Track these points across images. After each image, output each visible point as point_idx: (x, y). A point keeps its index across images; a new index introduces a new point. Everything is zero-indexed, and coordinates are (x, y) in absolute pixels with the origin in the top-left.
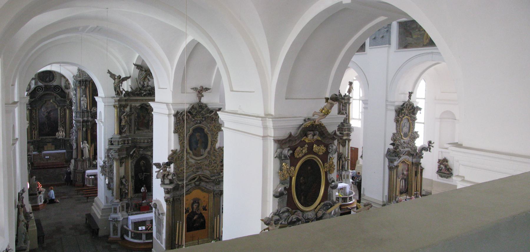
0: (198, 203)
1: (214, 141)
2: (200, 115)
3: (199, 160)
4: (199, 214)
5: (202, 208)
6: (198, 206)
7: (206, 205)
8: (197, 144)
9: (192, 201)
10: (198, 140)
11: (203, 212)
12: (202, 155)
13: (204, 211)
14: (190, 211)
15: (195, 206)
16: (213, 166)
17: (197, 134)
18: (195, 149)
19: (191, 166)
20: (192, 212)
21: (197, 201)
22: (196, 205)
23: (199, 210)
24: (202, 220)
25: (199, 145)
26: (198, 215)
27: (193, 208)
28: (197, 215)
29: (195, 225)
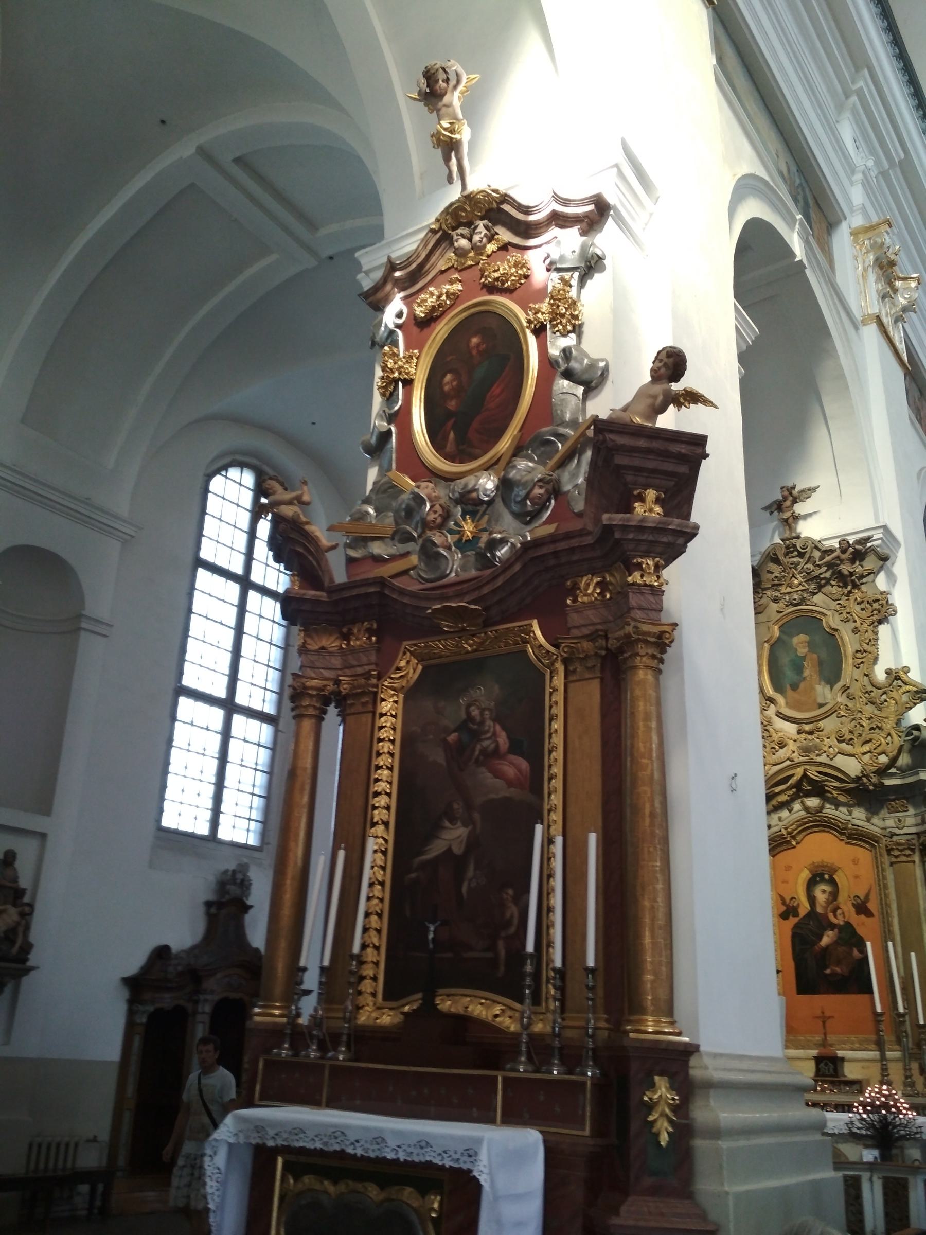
0: (832, 882)
1: (865, 651)
2: (798, 576)
3: (808, 721)
4: (841, 929)
5: (850, 904)
6: (834, 895)
7: (867, 896)
8: (798, 668)
9: (805, 875)
10: (804, 658)
11: (857, 921)
12: (821, 706)
13: (862, 917)
14: (803, 912)
15: (821, 893)
16: (870, 740)
17: (799, 641)
18: (795, 687)
19: (782, 745)
20: (812, 914)
21: (826, 877)
22: (824, 891)
23: (839, 911)
24: (856, 953)
25: (806, 673)
26: (836, 930)
27: (812, 900)
28: (832, 930)
29: (828, 971)
